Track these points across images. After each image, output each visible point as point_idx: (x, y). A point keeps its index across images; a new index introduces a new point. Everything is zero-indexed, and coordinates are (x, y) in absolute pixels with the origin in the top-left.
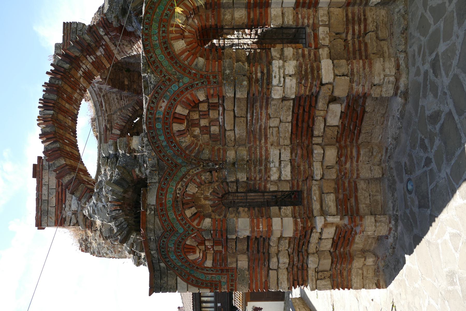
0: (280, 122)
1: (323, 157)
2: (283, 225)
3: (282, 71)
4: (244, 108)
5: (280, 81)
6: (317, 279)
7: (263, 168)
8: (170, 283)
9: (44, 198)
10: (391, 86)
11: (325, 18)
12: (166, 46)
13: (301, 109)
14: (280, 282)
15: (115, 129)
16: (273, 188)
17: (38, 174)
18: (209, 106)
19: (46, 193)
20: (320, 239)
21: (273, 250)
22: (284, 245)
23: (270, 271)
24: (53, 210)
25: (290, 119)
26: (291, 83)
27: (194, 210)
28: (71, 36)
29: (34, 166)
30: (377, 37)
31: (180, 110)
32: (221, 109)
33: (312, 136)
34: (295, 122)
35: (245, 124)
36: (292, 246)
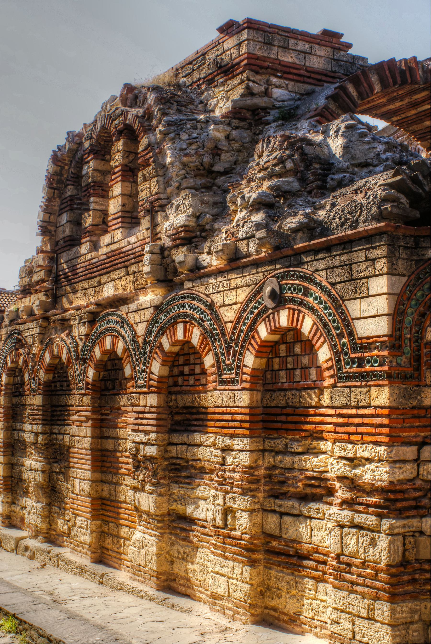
6: (404, 537)
9: (292, 41)
17: (327, 39)
29: (342, 35)
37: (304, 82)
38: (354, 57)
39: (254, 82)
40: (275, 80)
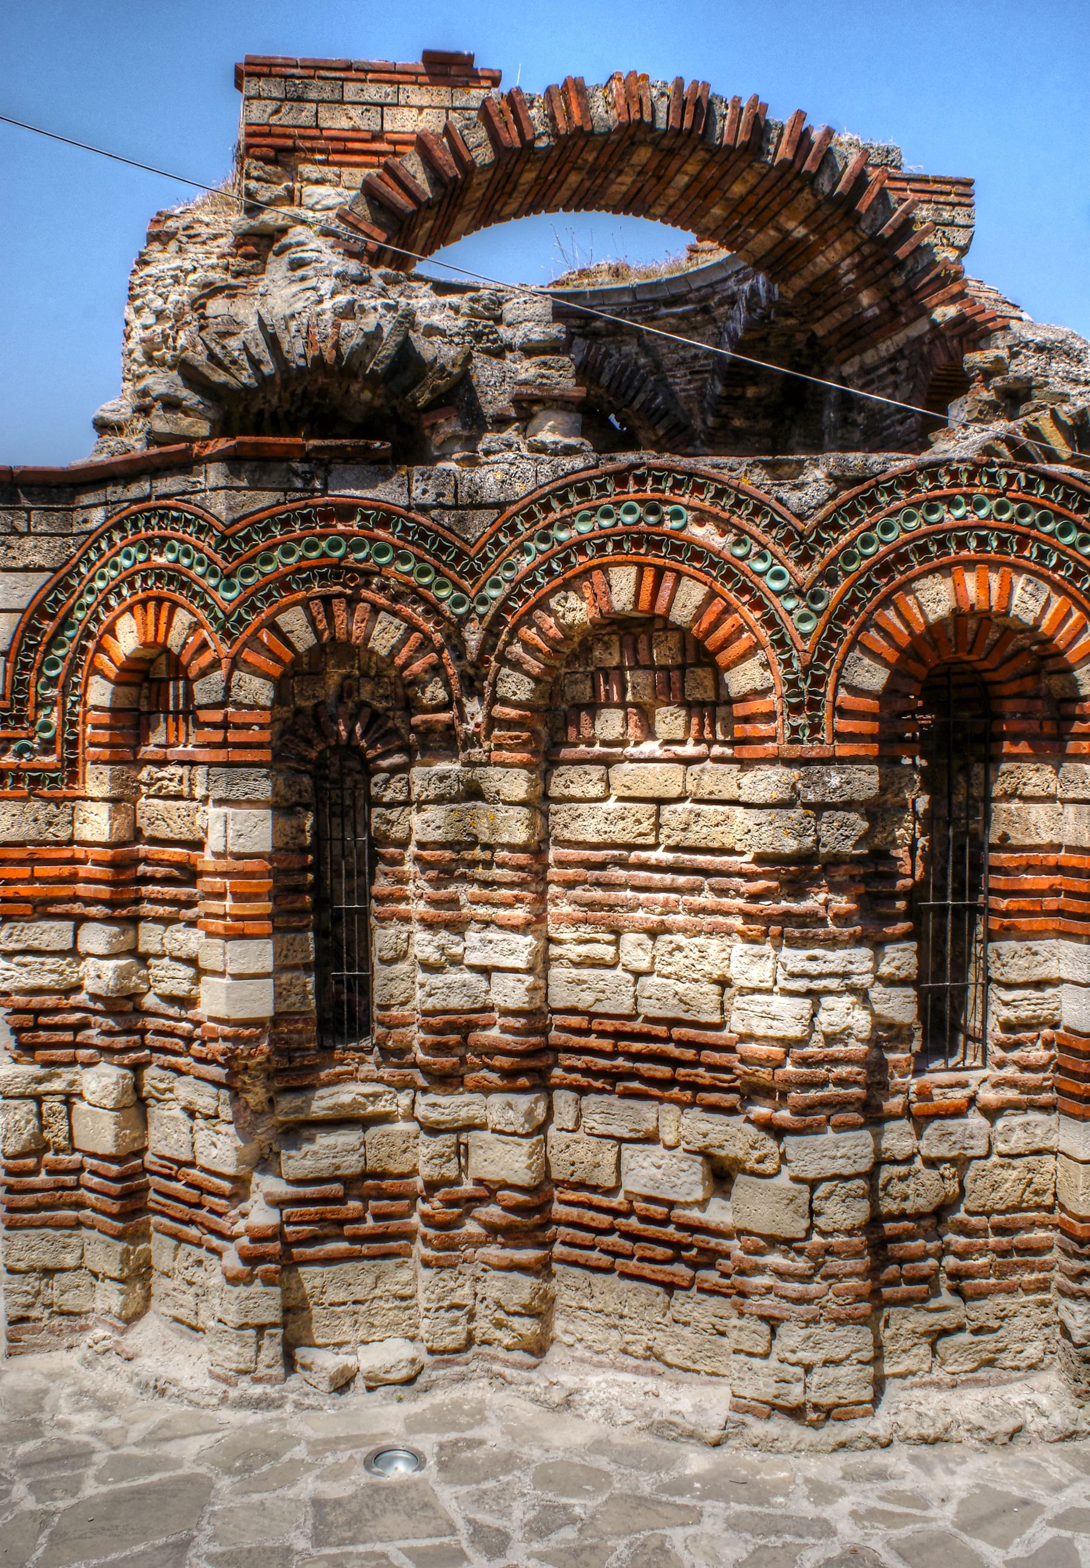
3: (833, 984)
13: (689, 1054)
14: (29, 959)
15: (589, 348)
19: (366, 97)
25: (648, 1008)
26: (785, 1016)
30: (945, 1333)
32: (690, 750)
33: (582, 1091)
34: (637, 1025)
35: (627, 838)
39: (258, 179)
40: (308, 170)
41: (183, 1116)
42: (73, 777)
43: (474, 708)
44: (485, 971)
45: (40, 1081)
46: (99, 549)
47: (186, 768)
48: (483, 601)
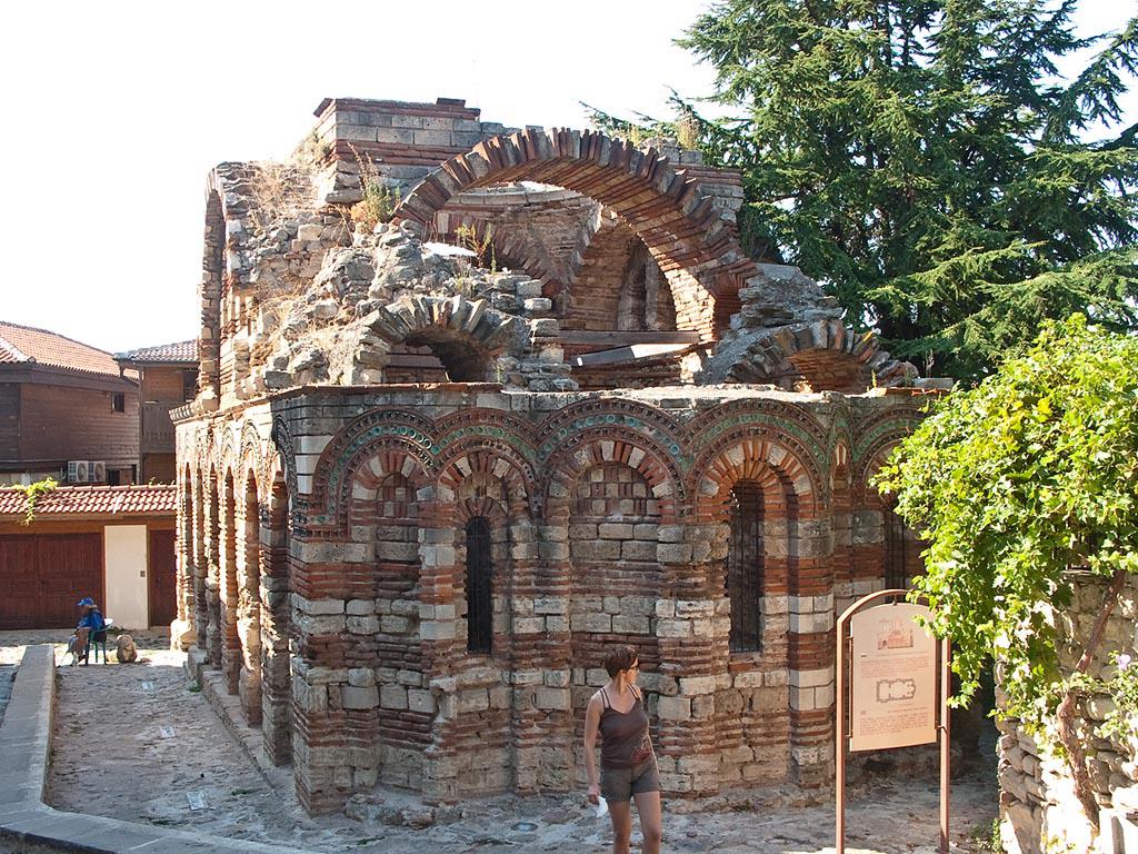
0: (613, 615)
1: (553, 687)
2: (444, 623)
3: (698, 615)
4: (636, 556)
5: (682, 612)
7: (533, 586)
8: (324, 422)
10: (676, 786)
11: (773, 682)
12: (737, 436)
14: (324, 618)
16: (498, 603)
18: (641, 499)
20: (407, 687)
21: (384, 605)
22: (398, 625)
23: (343, 601)
24: (372, 138)
25: (620, 630)
26: (681, 630)
27: (467, 471)
28: (716, 186)
31: (637, 456)
32: (636, 518)
34: (610, 638)
36: (391, 639)
37: (412, 164)
38: (482, 124)
39: (343, 172)
41: (402, 689)
42: (346, 532)
43: (539, 498)
44: (545, 616)
45: (328, 676)
46: (359, 425)
47: (406, 528)
48: (543, 453)
